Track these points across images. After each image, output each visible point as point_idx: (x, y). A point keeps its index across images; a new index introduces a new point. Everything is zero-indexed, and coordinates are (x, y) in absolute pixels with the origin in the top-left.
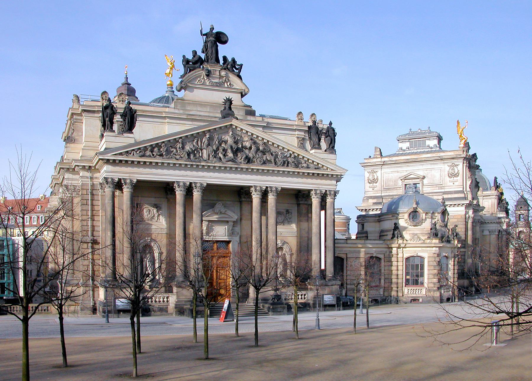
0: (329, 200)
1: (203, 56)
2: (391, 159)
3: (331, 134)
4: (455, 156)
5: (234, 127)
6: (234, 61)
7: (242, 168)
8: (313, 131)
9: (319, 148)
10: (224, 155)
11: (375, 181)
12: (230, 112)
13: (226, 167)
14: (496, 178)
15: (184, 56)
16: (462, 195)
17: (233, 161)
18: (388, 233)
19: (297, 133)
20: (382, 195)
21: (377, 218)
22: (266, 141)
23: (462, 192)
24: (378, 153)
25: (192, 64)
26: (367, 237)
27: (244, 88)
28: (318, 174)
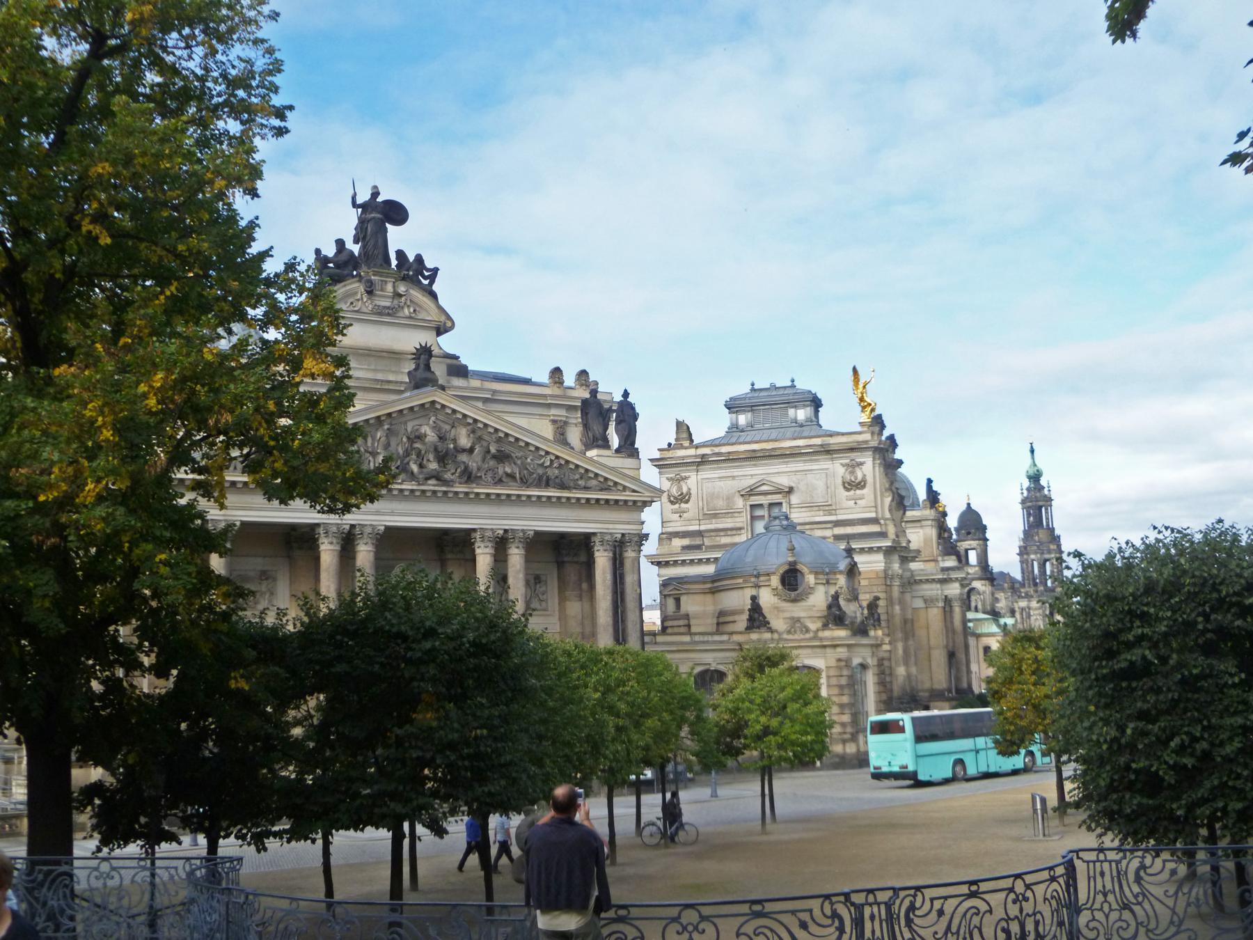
0: (629, 554)
1: (356, 249)
2: (717, 450)
3: (627, 415)
4: (855, 445)
5: (438, 406)
6: (419, 259)
7: (456, 493)
8: (592, 412)
9: (606, 444)
10: (421, 466)
11: (683, 498)
12: (428, 375)
13: (424, 492)
14: (930, 481)
15: (318, 252)
16: (875, 528)
17: (437, 477)
18: (736, 618)
19: (554, 411)
20: (703, 528)
21: (709, 586)
22: (502, 435)
23: (875, 521)
24: (685, 435)
26: (689, 626)
27: (443, 318)
28: (607, 501)
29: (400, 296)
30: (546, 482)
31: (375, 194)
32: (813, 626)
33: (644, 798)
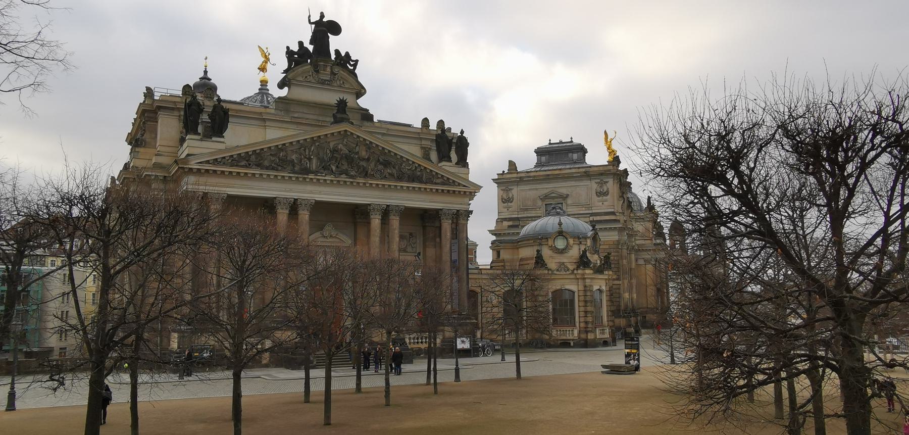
1: (311, 48)
3: (462, 144)
6: (347, 54)
7: (358, 183)
9: (450, 160)
13: (339, 181)
15: (288, 48)
16: (613, 217)
19: (424, 142)
23: (613, 213)
25: (297, 58)
28: (448, 191)
29: (335, 74)
30: (412, 179)
31: (322, 16)
32: (571, 267)
33: (143, 378)
